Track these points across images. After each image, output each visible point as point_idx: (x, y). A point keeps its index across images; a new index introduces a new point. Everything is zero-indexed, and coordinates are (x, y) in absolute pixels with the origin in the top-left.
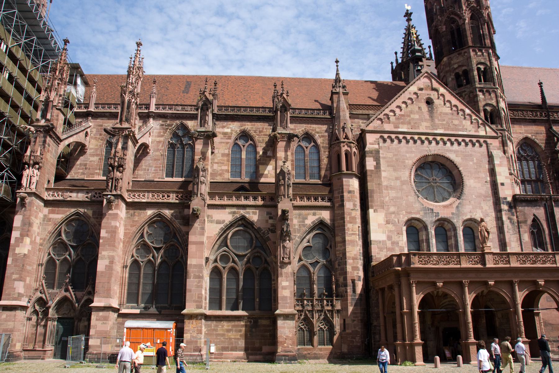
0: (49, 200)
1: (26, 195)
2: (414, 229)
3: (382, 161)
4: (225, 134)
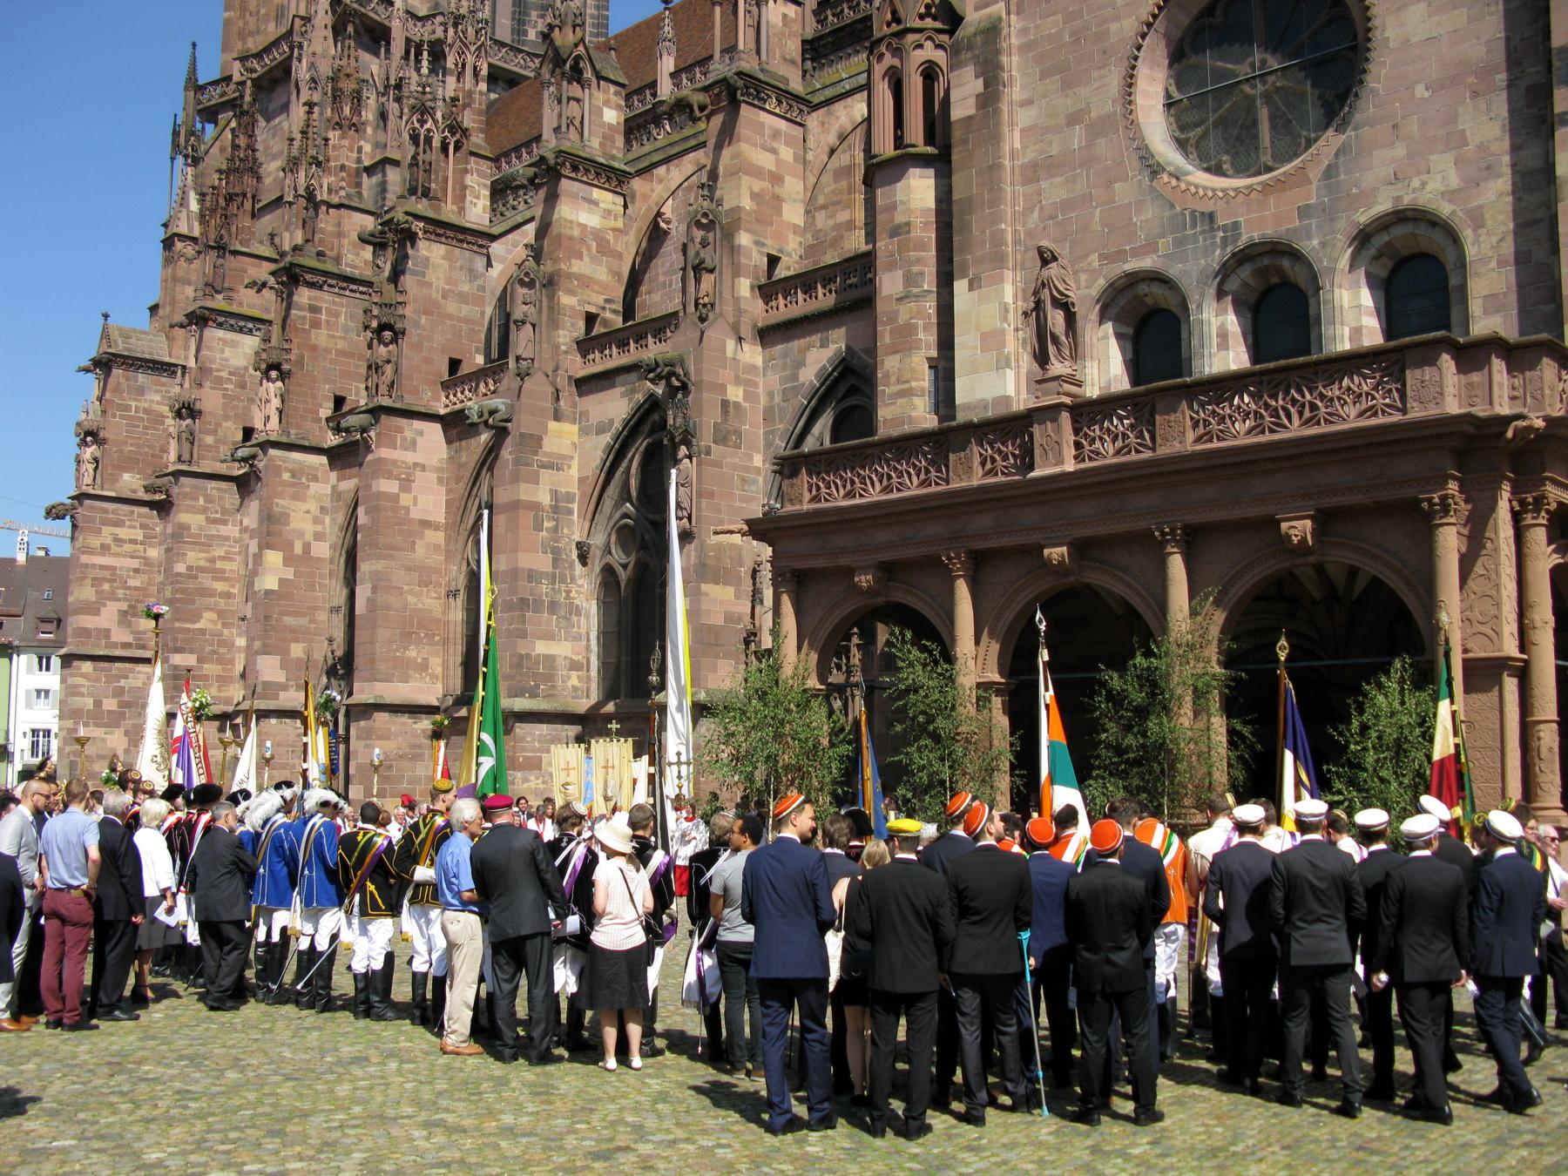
2: (1153, 324)
3: (1013, 64)
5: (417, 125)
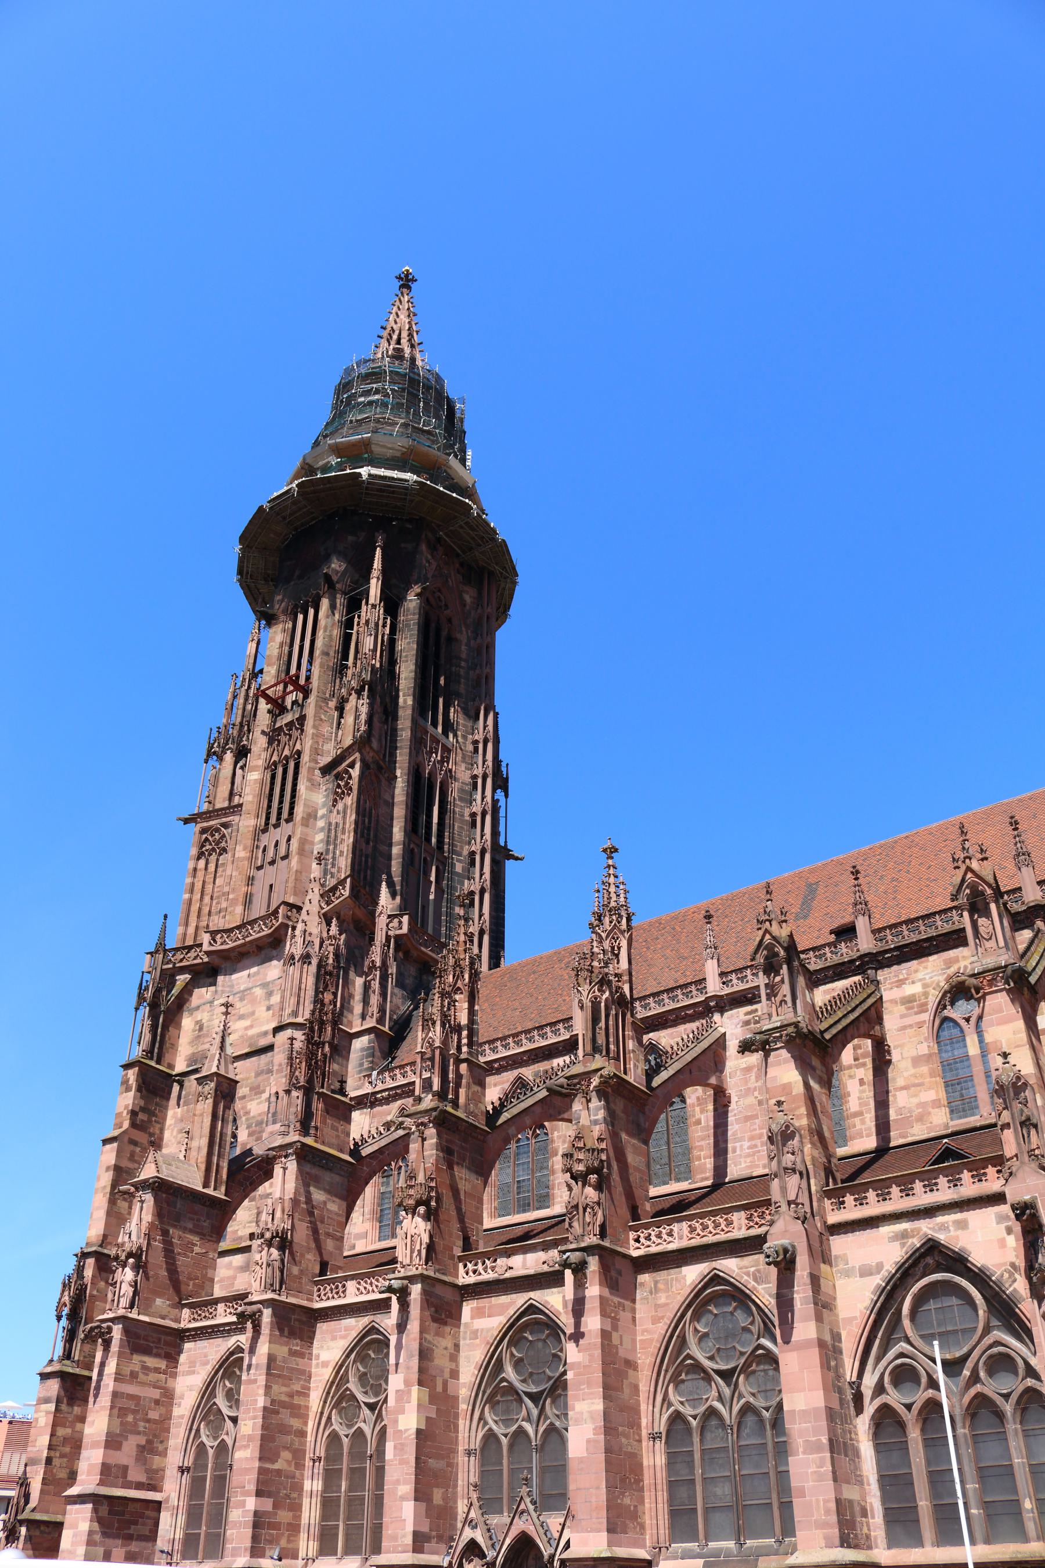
0: (469, 1285)
1: (406, 1282)
4: (908, 1001)
5: (597, 993)
